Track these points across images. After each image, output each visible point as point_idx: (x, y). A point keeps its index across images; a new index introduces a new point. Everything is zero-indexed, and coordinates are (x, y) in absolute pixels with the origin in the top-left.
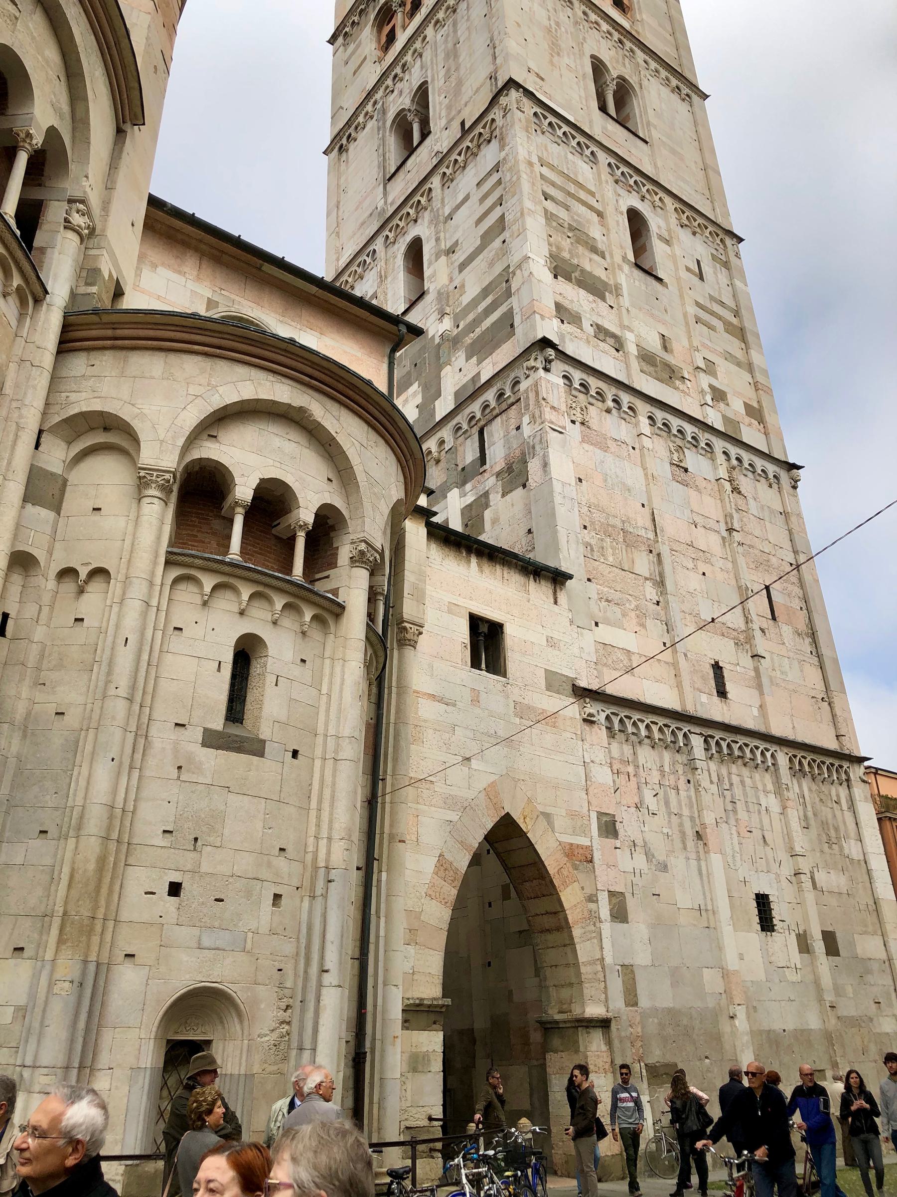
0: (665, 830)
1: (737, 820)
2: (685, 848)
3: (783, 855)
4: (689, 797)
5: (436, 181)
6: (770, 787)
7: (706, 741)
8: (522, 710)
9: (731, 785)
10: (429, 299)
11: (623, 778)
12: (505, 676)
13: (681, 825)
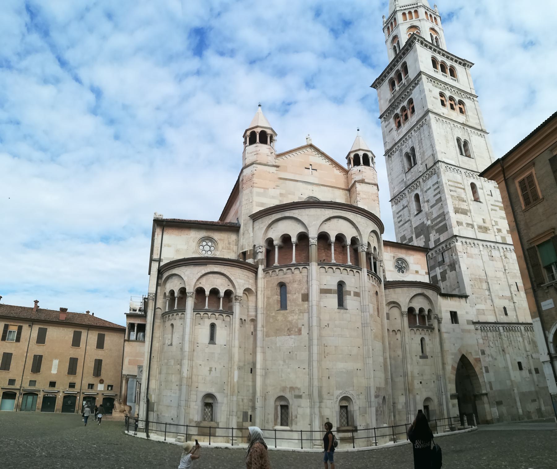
0: (495, 351)
1: (512, 345)
2: (500, 354)
3: (524, 352)
4: (500, 342)
5: (421, 180)
6: (520, 335)
7: (503, 328)
8: (463, 331)
9: (510, 337)
10: (423, 213)
11: (485, 340)
12: (458, 324)
13: (499, 349)
